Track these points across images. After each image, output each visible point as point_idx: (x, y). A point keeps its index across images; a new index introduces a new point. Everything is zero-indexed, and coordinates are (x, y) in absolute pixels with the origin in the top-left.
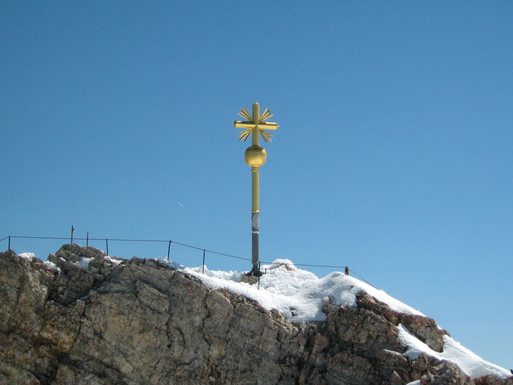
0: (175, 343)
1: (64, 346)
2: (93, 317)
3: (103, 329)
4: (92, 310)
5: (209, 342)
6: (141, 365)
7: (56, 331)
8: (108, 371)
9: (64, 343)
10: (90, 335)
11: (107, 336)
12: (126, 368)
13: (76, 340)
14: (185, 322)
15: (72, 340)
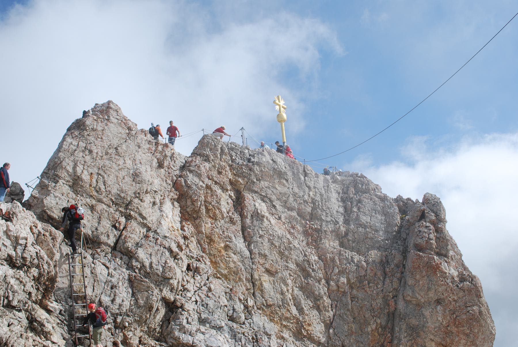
0: (295, 188)
1: (241, 186)
2: (256, 172)
3: (261, 178)
4: (255, 168)
5: (309, 188)
6: (281, 196)
7: (237, 178)
8: (266, 199)
9: (241, 184)
10: (255, 180)
11: (262, 182)
12: (274, 197)
13: (247, 183)
14: (296, 179)
15: (245, 183)
